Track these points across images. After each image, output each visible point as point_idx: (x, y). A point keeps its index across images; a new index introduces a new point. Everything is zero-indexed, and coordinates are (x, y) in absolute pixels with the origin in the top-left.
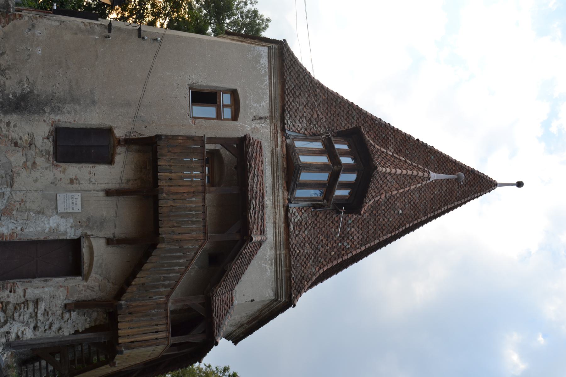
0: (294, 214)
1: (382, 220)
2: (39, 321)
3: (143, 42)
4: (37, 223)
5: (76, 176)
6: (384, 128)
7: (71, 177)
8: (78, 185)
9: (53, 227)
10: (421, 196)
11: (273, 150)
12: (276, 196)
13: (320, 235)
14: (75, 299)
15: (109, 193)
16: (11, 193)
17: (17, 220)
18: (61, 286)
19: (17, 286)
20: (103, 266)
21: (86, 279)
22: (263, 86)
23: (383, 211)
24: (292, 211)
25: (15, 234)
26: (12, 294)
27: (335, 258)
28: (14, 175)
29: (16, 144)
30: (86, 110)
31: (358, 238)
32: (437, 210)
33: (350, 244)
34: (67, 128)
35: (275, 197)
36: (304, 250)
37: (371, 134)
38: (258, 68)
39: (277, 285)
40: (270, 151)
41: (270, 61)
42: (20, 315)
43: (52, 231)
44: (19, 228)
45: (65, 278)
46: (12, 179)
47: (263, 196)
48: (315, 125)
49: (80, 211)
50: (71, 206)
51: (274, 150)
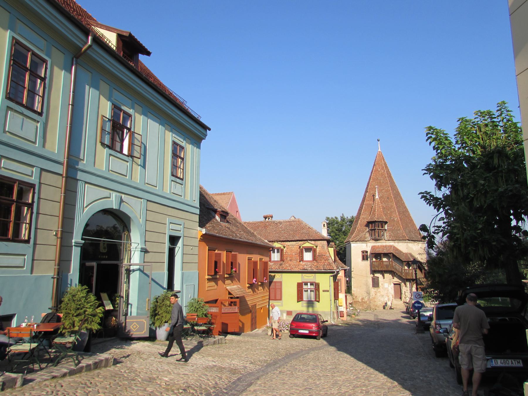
43: (391, 289)
47: (383, 246)
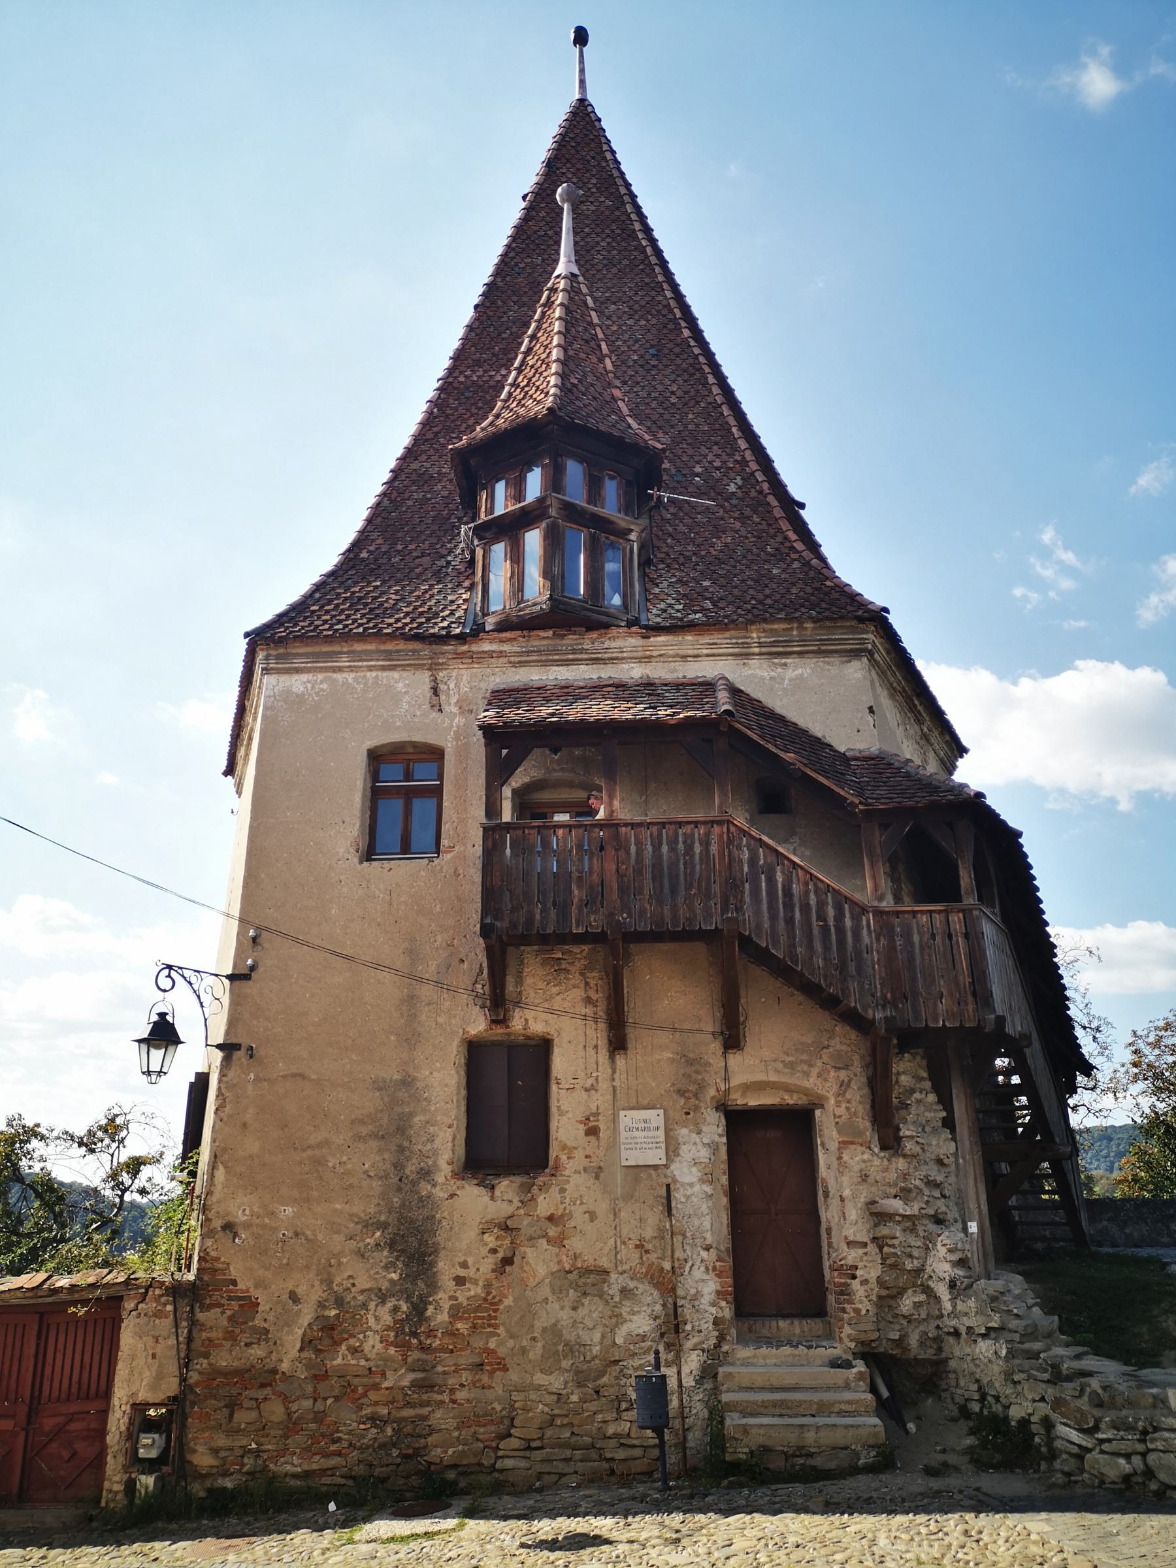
0: (664, 611)
1: (673, 397)
2: (923, 1212)
3: (261, 969)
4: (691, 1212)
5: (581, 1122)
6: (449, 394)
7: (582, 1132)
8: (600, 1118)
9: (700, 1174)
10: (613, 299)
11: (510, 663)
12: (620, 655)
13: (712, 550)
14: (868, 1124)
15: (618, 1043)
16: (621, 1274)
17: (686, 1261)
18: (839, 1158)
19: (840, 1260)
20: (790, 1059)
21: (818, 1103)
22: (360, 687)
23: (653, 395)
24: (658, 615)
25: (718, 1264)
26: (859, 1273)
27: (769, 512)
28: (579, 1265)
29: (508, 1261)
30: (426, 1099)
31: (717, 456)
32: (647, 257)
33: (732, 475)
34: (466, 1143)
35: (624, 658)
36: (750, 587)
37: (464, 425)
38: (316, 698)
39: (836, 651)
40: (514, 669)
41: (298, 671)
42: (910, 1256)
43: (708, 1178)
44: (704, 1254)
45: (819, 1148)
46: (588, 1271)
48: (449, 563)
49: (661, 1112)
50: (651, 1134)
51: (512, 659)
